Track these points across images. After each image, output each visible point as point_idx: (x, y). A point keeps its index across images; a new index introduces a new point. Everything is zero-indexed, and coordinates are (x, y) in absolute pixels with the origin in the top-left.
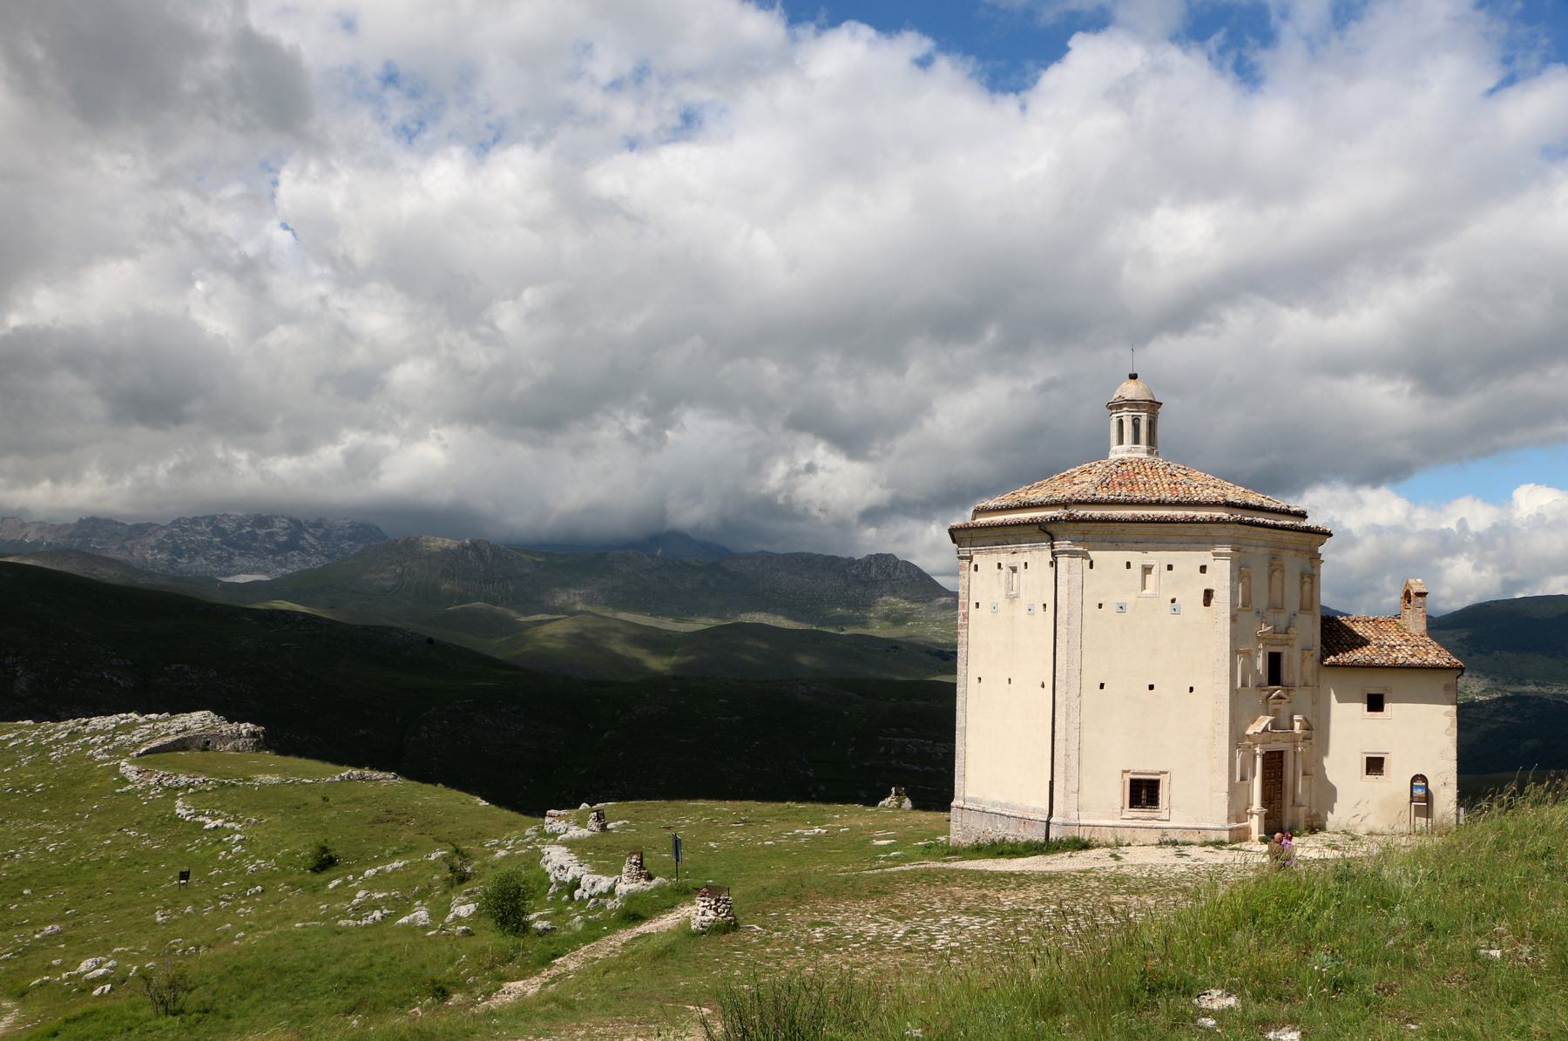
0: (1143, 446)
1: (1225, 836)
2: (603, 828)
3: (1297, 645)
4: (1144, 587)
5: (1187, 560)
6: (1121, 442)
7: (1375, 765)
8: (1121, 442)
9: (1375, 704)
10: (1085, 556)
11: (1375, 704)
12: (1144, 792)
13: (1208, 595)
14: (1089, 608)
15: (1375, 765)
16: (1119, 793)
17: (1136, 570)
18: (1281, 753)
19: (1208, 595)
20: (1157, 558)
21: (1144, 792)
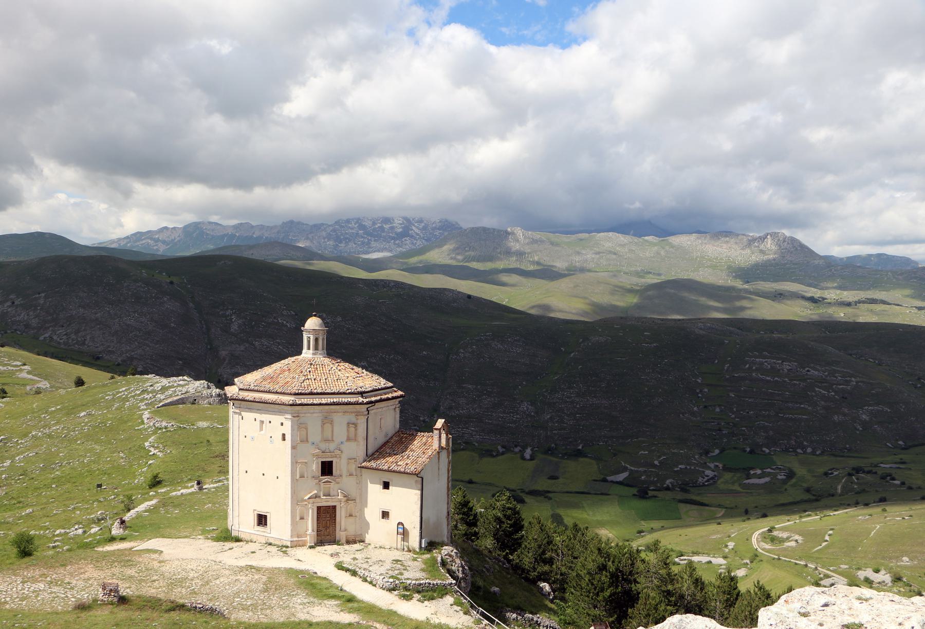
0: (311, 351)
1: (289, 544)
2: (201, 489)
3: (344, 457)
4: (261, 429)
5: (277, 419)
6: (309, 348)
7: (385, 515)
8: (309, 348)
9: (386, 486)
10: (240, 414)
11: (386, 486)
12: (262, 520)
13: (284, 435)
14: (242, 437)
15: (385, 515)
16: (253, 520)
17: (258, 422)
18: (334, 507)
19: (284, 435)
20: (266, 417)
21: (262, 520)
